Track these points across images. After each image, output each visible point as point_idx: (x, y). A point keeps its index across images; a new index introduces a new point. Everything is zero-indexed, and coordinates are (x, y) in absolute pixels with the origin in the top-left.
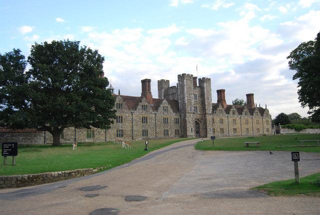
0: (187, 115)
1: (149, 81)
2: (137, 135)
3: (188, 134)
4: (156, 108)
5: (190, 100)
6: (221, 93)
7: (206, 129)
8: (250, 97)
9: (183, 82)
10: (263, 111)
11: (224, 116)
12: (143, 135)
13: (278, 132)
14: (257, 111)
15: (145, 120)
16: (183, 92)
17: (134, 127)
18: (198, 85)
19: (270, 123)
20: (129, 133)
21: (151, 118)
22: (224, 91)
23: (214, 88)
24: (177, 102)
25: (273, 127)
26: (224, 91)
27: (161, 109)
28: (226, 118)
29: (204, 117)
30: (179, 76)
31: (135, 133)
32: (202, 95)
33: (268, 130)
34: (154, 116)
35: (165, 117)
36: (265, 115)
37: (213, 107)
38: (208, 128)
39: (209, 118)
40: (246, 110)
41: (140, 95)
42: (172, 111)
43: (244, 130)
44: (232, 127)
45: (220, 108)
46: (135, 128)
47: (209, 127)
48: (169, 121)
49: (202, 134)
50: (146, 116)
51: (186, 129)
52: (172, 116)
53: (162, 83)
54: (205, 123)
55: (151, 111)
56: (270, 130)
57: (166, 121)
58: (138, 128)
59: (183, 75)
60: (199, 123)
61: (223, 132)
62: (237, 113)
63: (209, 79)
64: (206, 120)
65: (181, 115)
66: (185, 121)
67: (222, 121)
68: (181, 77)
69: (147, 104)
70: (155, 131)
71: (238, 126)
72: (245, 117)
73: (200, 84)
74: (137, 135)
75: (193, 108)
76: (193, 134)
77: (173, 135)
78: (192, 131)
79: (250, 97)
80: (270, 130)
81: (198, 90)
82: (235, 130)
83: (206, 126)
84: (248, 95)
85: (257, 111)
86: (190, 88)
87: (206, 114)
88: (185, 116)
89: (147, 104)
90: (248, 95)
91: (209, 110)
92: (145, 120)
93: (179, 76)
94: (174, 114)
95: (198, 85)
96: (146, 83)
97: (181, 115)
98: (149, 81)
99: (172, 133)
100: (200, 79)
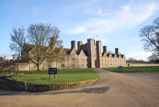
0: (92, 57)
6: (105, 48)
7: (100, 64)
8: (117, 50)
10: (122, 56)
11: (107, 58)
13: (129, 65)
14: (120, 56)
16: (90, 47)
19: (125, 61)
25: (127, 63)
28: (107, 59)
30: (88, 39)
33: (125, 65)
36: (123, 58)
39: (101, 59)
40: (116, 56)
43: (115, 64)
44: (110, 63)
56: (125, 64)
62: (112, 57)
65: (89, 57)
67: (106, 60)
71: (112, 63)
72: (115, 58)
79: (117, 50)
80: (125, 64)
81: (96, 46)
82: (111, 64)
84: (115, 49)
85: (120, 56)
86: (93, 45)
90: (115, 49)
91: (101, 55)
100: (96, 41)
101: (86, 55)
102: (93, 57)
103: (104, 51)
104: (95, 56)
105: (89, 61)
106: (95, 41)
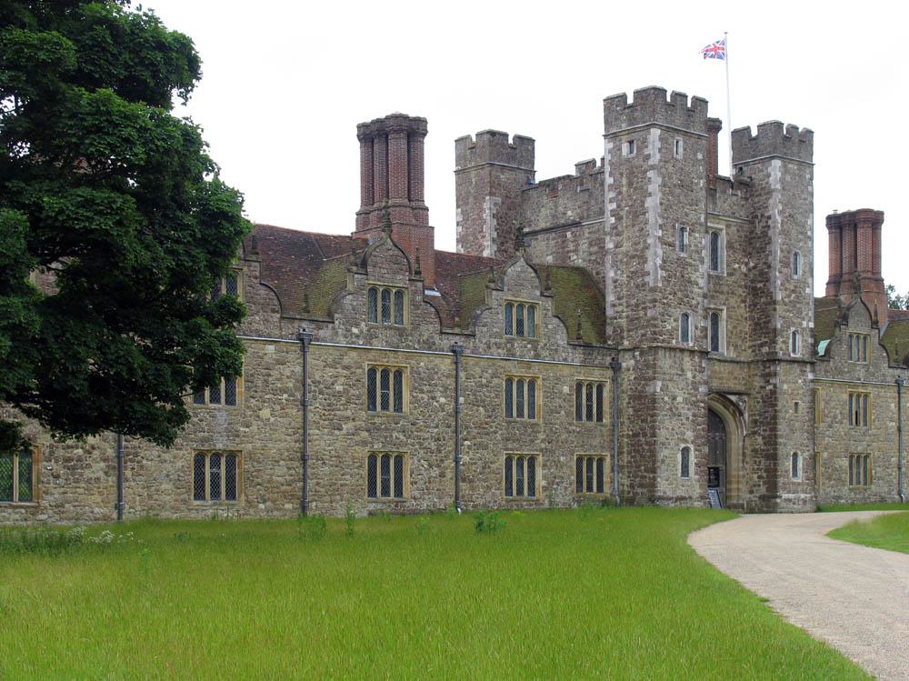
1: (410, 131)
2: (334, 489)
3: (663, 487)
4: (458, 317)
5: (682, 264)
6: (856, 229)
7: (773, 457)
9: (637, 143)
12: (372, 492)
15: (382, 387)
17: (313, 431)
18: (725, 169)
20: (281, 473)
21: (421, 380)
22: (872, 220)
23: (833, 193)
24: (589, 287)
26: (872, 220)
27: (493, 320)
28: (892, 393)
29: (758, 382)
31: (322, 472)
32: (754, 240)
34: (445, 365)
35: (517, 371)
37: (817, 315)
38: (781, 451)
39: (791, 384)
41: (344, 224)
42: (561, 339)
45: (858, 326)
46: (321, 441)
47: (792, 444)
48: (540, 399)
49: (742, 472)
50: (392, 362)
51: (653, 454)
52: (561, 367)
53: (498, 160)
54: (768, 422)
55: (429, 329)
57: (518, 394)
58: (342, 444)
59: (650, 96)
60: (727, 415)
61: (868, 479)
63: (809, 133)
64: (771, 399)
66: (645, 406)
68: (644, 114)
69: (401, 280)
70: (450, 463)
73: (738, 166)
74: (334, 489)
75: (697, 322)
76: (694, 484)
77: (564, 494)
78: (685, 471)
83: (772, 440)
86: (686, 186)
87: (774, 360)
88: (647, 373)
89: (401, 280)
92: (382, 387)
93: (615, 106)
94: (577, 357)
95: (725, 169)
96: (391, 145)
97: (616, 367)
98: (410, 131)
99: (554, 478)
100: (740, 135)
101: (578, 342)
102: (687, 362)
103: (835, 282)
104: (704, 353)
105: (617, 413)
106: (715, 126)
